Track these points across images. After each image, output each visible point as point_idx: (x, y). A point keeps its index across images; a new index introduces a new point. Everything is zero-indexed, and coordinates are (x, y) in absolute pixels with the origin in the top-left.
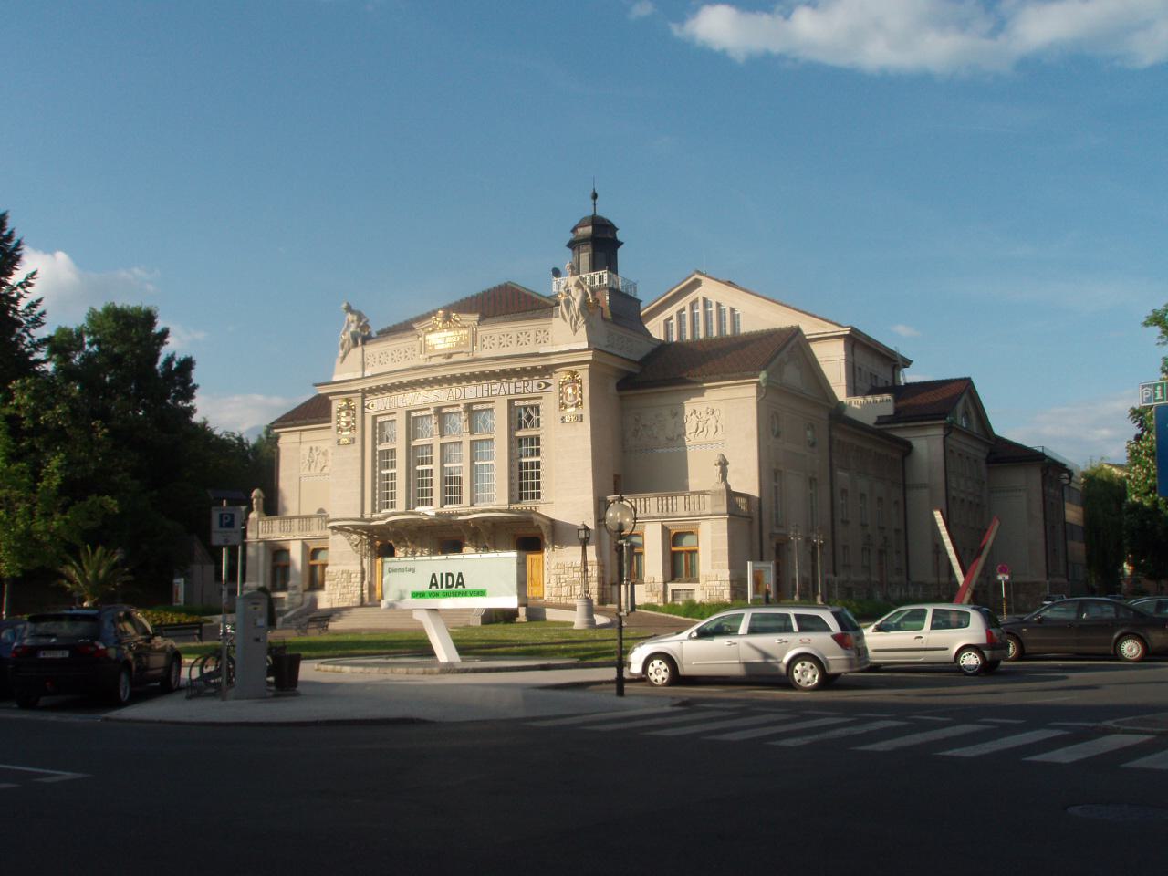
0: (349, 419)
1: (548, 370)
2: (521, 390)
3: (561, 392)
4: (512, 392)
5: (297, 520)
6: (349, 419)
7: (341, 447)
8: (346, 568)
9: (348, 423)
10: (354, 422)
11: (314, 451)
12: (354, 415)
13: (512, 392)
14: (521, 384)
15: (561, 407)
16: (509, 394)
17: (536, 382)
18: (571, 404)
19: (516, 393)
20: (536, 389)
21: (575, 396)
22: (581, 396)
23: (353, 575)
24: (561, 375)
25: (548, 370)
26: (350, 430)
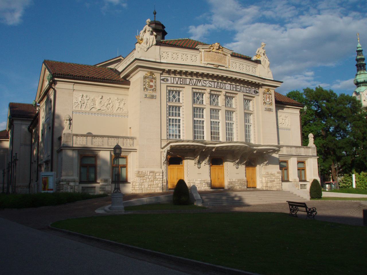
0: (151, 84)
1: (258, 86)
2: (248, 92)
3: (264, 97)
4: (245, 92)
5: (107, 138)
6: (151, 84)
7: (146, 99)
8: (152, 170)
9: (151, 86)
10: (155, 86)
11: (84, 97)
12: (155, 82)
13: (245, 92)
14: (247, 89)
15: (264, 103)
16: (244, 92)
17: (253, 90)
18: (268, 103)
19: (246, 93)
20: (253, 93)
21: (270, 99)
22: (272, 100)
23: (157, 174)
24: (261, 90)
25: (258, 86)
26: (153, 90)
